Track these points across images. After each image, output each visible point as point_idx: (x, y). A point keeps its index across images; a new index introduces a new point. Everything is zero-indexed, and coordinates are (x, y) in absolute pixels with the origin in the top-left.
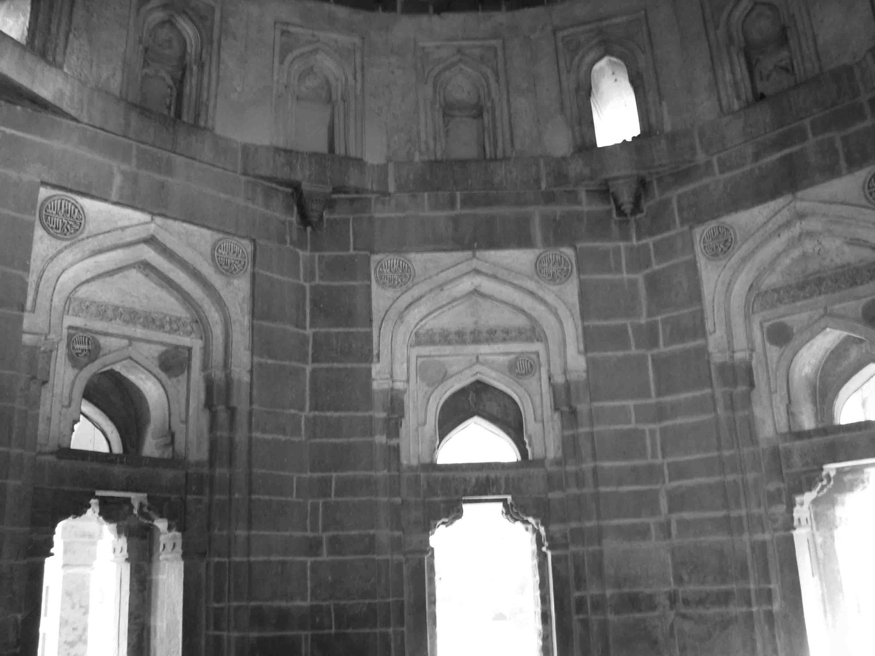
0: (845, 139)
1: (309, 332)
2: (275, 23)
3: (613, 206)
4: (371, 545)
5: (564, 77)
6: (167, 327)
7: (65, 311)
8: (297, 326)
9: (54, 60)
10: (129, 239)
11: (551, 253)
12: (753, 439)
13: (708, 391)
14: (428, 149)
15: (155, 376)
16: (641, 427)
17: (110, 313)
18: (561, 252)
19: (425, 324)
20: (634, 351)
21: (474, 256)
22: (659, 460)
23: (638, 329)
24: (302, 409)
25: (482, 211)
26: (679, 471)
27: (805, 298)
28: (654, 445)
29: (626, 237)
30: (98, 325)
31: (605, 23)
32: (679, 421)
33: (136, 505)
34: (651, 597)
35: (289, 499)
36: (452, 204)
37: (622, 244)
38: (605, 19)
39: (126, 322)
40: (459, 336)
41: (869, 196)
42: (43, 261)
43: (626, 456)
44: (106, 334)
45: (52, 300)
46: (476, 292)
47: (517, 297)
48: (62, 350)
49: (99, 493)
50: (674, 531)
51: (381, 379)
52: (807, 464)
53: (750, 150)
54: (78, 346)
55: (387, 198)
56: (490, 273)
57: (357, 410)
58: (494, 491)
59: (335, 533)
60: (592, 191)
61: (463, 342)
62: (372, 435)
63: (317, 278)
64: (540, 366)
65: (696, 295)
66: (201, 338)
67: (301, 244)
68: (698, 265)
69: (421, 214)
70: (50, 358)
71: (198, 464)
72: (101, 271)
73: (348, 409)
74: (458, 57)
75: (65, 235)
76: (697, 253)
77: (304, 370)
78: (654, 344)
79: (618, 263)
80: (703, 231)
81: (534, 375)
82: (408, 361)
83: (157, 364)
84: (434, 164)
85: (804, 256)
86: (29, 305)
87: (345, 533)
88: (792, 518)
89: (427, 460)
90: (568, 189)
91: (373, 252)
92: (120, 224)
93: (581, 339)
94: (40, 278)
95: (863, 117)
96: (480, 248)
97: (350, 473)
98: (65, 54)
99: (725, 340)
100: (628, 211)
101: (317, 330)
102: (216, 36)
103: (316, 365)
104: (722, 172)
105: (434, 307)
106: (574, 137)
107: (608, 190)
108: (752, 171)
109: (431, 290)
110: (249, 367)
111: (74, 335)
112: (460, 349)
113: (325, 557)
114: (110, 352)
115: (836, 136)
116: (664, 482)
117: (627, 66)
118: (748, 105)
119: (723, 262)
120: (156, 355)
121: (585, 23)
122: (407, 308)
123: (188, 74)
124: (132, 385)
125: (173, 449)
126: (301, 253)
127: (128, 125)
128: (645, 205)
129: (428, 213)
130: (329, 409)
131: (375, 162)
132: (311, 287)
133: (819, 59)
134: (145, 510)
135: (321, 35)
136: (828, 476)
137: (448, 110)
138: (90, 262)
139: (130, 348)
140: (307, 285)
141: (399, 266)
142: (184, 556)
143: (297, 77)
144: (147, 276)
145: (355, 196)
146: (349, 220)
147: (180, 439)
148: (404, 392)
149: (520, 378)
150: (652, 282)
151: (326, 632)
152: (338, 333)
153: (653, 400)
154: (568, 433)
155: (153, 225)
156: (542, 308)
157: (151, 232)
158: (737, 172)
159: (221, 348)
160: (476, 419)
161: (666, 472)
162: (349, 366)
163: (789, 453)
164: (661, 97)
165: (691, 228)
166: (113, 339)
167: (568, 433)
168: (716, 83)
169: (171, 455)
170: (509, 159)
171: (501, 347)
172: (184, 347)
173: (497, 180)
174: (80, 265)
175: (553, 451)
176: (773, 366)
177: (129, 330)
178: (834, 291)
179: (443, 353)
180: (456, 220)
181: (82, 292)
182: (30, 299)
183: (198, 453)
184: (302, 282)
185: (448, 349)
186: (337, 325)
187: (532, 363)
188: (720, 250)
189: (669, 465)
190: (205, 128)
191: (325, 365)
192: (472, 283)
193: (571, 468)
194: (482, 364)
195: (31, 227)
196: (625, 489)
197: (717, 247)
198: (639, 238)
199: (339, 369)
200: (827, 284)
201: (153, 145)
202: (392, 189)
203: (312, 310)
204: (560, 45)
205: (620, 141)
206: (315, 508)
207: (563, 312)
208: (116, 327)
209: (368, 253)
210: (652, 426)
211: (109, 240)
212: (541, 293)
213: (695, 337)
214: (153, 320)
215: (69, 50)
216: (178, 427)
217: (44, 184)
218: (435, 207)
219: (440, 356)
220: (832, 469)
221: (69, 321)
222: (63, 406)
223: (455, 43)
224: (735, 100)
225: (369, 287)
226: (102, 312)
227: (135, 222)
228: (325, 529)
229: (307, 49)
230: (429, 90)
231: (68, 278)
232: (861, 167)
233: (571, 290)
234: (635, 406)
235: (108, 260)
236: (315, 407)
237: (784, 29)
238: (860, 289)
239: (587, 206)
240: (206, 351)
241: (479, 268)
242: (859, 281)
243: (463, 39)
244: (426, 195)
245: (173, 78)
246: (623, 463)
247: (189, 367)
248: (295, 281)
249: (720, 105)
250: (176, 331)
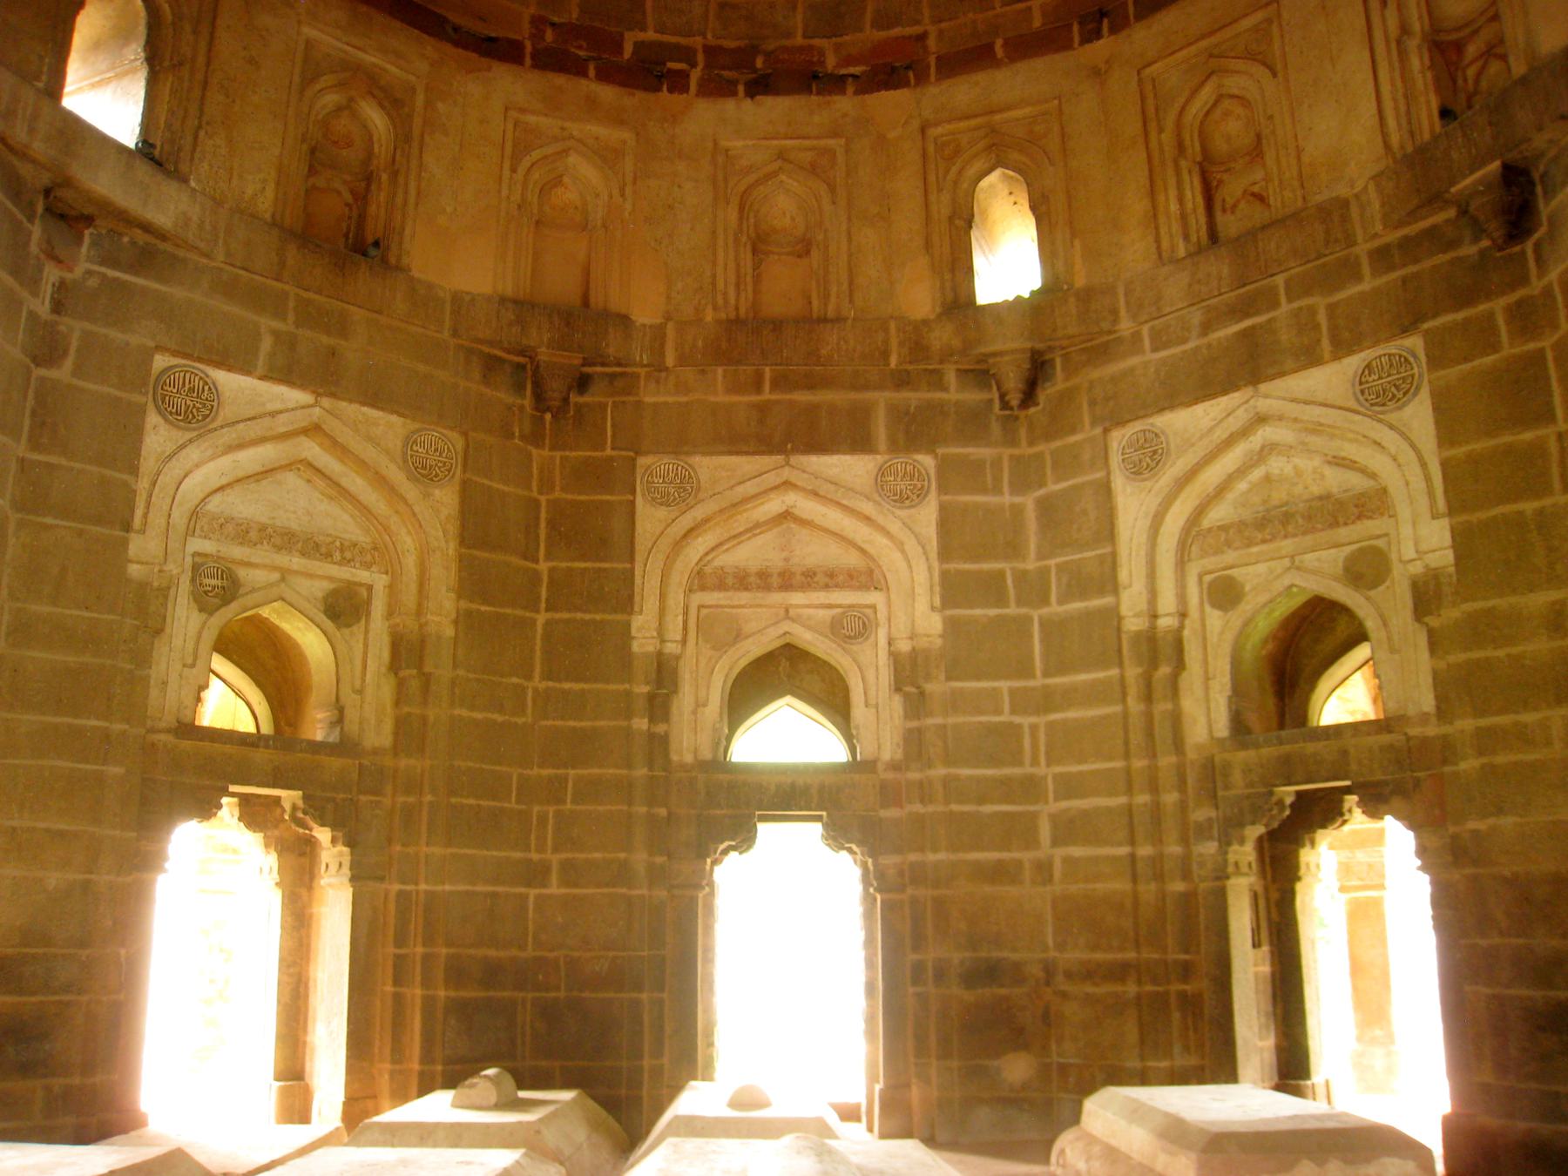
0: (1331, 308)
1: (543, 567)
2: (507, 109)
3: (996, 396)
4: (622, 874)
5: (933, 198)
6: (337, 556)
7: (190, 532)
8: (525, 558)
9: (176, 170)
10: (282, 430)
11: (899, 461)
12: (1178, 744)
13: (1114, 672)
14: (726, 301)
15: (318, 626)
16: (1017, 719)
17: (253, 535)
18: (915, 461)
19: (713, 559)
20: (1012, 610)
21: (787, 463)
22: (1041, 770)
23: (1021, 577)
24: (529, 677)
25: (803, 397)
26: (1068, 786)
27: (1264, 541)
28: (1035, 746)
29: (1012, 441)
30: (237, 552)
31: (998, 117)
32: (1071, 714)
33: (287, 806)
34: (1017, 966)
35: (506, 805)
36: (758, 388)
37: (1007, 452)
38: (1001, 111)
39: (279, 549)
40: (761, 578)
41: (1359, 394)
42: (157, 461)
43: (994, 761)
44: (249, 564)
45: (170, 515)
46: (786, 516)
47: (847, 525)
48: (185, 585)
49: (233, 788)
50: (1057, 874)
52: (1250, 785)
53: (1196, 317)
54: (207, 581)
55: (663, 374)
56: (810, 488)
57: (608, 681)
58: (802, 803)
59: (569, 855)
60: (966, 371)
61: (767, 588)
62: (629, 717)
63: (557, 488)
64: (877, 625)
65: (1108, 531)
66: (387, 573)
67: (536, 438)
68: (1113, 485)
69: (712, 399)
70: (166, 597)
71: (376, 752)
72: (241, 474)
73: (596, 681)
74: (779, 163)
75: (190, 423)
76: (1112, 468)
77: (534, 622)
78: (1045, 601)
79: (997, 480)
80: (1124, 436)
81: (867, 638)
82: (686, 614)
83: (322, 609)
84: (734, 324)
85: (1267, 478)
86: (137, 522)
87: (582, 856)
88: (1226, 861)
89: (706, 754)
90: (931, 367)
91: (637, 453)
92: (270, 407)
93: (937, 589)
94: (154, 484)
95: (1357, 277)
96: (797, 450)
97: (596, 771)
98: (192, 159)
99: (1144, 598)
100: (1015, 403)
101: (554, 564)
102: (416, 132)
103: (549, 615)
104: (1155, 349)
105: (726, 536)
106: (942, 288)
107: (986, 372)
108: (1197, 350)
109: (721, 511)
110: (454, 616)
111: (202, 565)
112: (758, 597)
113: (555, 889)
114: (253, 590)
115: (1319, 302)
116: (1047, 802)
117: (1028, 184)
118: (1200, 250)
119: (1148, 484)
120: (320, 595)
121: (967, 117)
122: (685, 536)
123: (373, 187)
124: (289, 638)
125: (342, 729)
126: (534, 451)
127: (282, 264)
128: (1045, 394)
129: (722, 398)
130: (567, 680)
131: (647, 321)
132: (548, 501)
133: (1302, 186)
134: (300, 815)
135: (575, 128)
136: (1280, 803)
137: (760, 244)
138: (225, 462)
139: (283, 585)
140: (543, 499)
141: (677, 474)
142: (354, 879)
143: (537, 191)
145: (618, 369)
146: (606, 405)
147: (351, 714)
148: (678, 658)
149: (845, 642)
150: (1046, 508)
151: (552, 994)
152: (585, 569)
153: (1038, 681)
154: (914, 724)
155: (317, 410)
156: (882, 540)
157: (315, 419)
158: (1176, 350)
159: (414, 587)
160: (788, 699)
161: (1051, 787)
162: (598, 617)
163: (1227, 766)
164: (1074, 235)
165: (1106, 431)
166: (258, 572)
167: (914, 724)
168: (1155, 216)
169: (338, 738)
170: (845, 320)
172: (361, 585)
173: (824, 352)
174: (212, 465)
175: (889, 749)
176: (1213, 638)
177: (283, 560)
178: (1304, 533)
179: (736, 603)
180: (763, 409)
181: (214, 505)
182: (139, 513)
183: (378, 735)
184: (535, 494)
185: (744, 597)
186: (583, 558)
187: (865, 620)
188: (1145, 464)
189: (1055, 777)
190: (398, 268)
191: (565, 615)
192: (783, 502)
193: (914, 776)
194: (793, 620)
195: (142, 411)
196: (988, 809)
197: (1140, 461)
198: (1031, 443)
199: (586, 623)
200: (1297, 522)
201: (319, 292)
202: (670, 361)
203: (549, 537)
204: (931, 149)
205: (1011, 298)
206: (543, 820)
207: (911, 546)
208: (262, 554)
209: (632, 454)
210: (1033, 720)
211: (254, 429)
212: (881, 520)
213: (1101, 592)
214: (317, 546)
215: (197, 155)
216: (349, 698)
217: (159, 348)
218: (735, 387)
219: (733, 607)
220: (1288, 793)
221: (197, 545)
222: (184, 666)
223: (775, 142)
224: (1181, 241)
225: (633, 503)
226: (244, 533)
227: (291, 405)
228: (556, 849)
229: (549, 150)
230: (733, 215)
232: (1350, 352)
233: (927, 515)
234: (1012, 692)
236: (548, 676)
237: (1259, 137)
238: (1343, 533)
239: (956, 393)
240: (391, 588)
241: (793, 480)
242: (1341, 520)
243: (786, 138)
244: (720, 370)
245: (352, 192)
246: (989, 772)
247: (368, 614)
248: (526, 493)
249: (1159, 248)
250: (349, 561)
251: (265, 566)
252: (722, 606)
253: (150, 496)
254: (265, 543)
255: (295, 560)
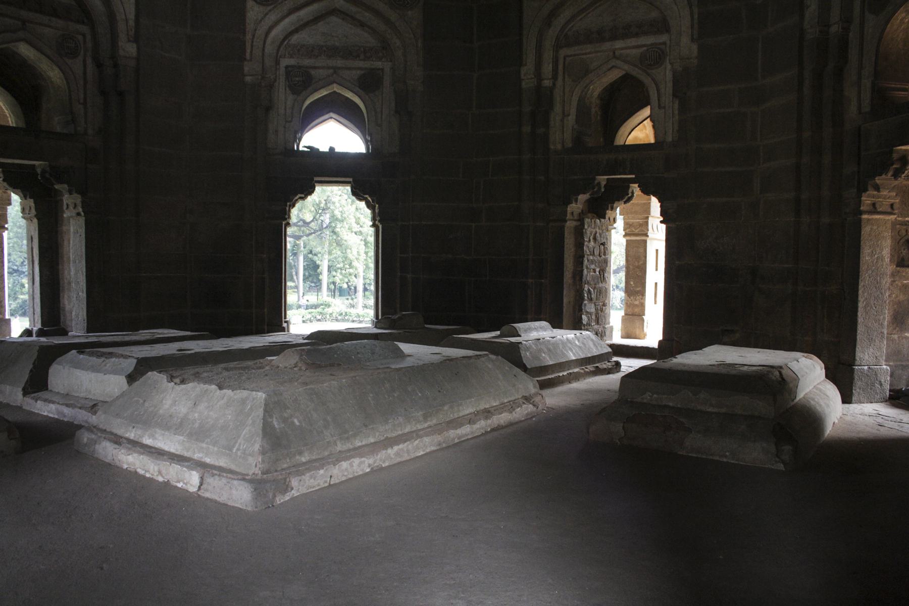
6: (362, 57)
30: (307, 62)
44: (315, 68)
51: (528, 79)
86: (248, 56)
94: (254, 36)
138: (293, 17)
144: (343, 19)
166: (321, 71)
171: (632, 42)
174: (287, 20)
177: (331, 62)
182: (248, 51)
194: (618, 58)
221: (285, 62)
226: (311, 51)
231: (277, 32)
235: (305, 13)
251: (323, 68)
252: (578, 55)
253: (253, 42)
254: (322, 55)
255: (339, 62)
